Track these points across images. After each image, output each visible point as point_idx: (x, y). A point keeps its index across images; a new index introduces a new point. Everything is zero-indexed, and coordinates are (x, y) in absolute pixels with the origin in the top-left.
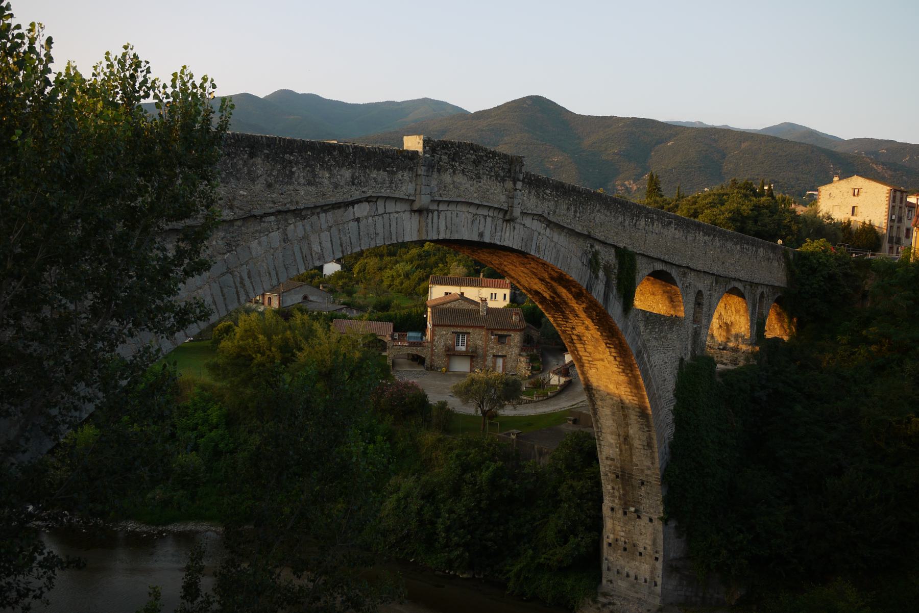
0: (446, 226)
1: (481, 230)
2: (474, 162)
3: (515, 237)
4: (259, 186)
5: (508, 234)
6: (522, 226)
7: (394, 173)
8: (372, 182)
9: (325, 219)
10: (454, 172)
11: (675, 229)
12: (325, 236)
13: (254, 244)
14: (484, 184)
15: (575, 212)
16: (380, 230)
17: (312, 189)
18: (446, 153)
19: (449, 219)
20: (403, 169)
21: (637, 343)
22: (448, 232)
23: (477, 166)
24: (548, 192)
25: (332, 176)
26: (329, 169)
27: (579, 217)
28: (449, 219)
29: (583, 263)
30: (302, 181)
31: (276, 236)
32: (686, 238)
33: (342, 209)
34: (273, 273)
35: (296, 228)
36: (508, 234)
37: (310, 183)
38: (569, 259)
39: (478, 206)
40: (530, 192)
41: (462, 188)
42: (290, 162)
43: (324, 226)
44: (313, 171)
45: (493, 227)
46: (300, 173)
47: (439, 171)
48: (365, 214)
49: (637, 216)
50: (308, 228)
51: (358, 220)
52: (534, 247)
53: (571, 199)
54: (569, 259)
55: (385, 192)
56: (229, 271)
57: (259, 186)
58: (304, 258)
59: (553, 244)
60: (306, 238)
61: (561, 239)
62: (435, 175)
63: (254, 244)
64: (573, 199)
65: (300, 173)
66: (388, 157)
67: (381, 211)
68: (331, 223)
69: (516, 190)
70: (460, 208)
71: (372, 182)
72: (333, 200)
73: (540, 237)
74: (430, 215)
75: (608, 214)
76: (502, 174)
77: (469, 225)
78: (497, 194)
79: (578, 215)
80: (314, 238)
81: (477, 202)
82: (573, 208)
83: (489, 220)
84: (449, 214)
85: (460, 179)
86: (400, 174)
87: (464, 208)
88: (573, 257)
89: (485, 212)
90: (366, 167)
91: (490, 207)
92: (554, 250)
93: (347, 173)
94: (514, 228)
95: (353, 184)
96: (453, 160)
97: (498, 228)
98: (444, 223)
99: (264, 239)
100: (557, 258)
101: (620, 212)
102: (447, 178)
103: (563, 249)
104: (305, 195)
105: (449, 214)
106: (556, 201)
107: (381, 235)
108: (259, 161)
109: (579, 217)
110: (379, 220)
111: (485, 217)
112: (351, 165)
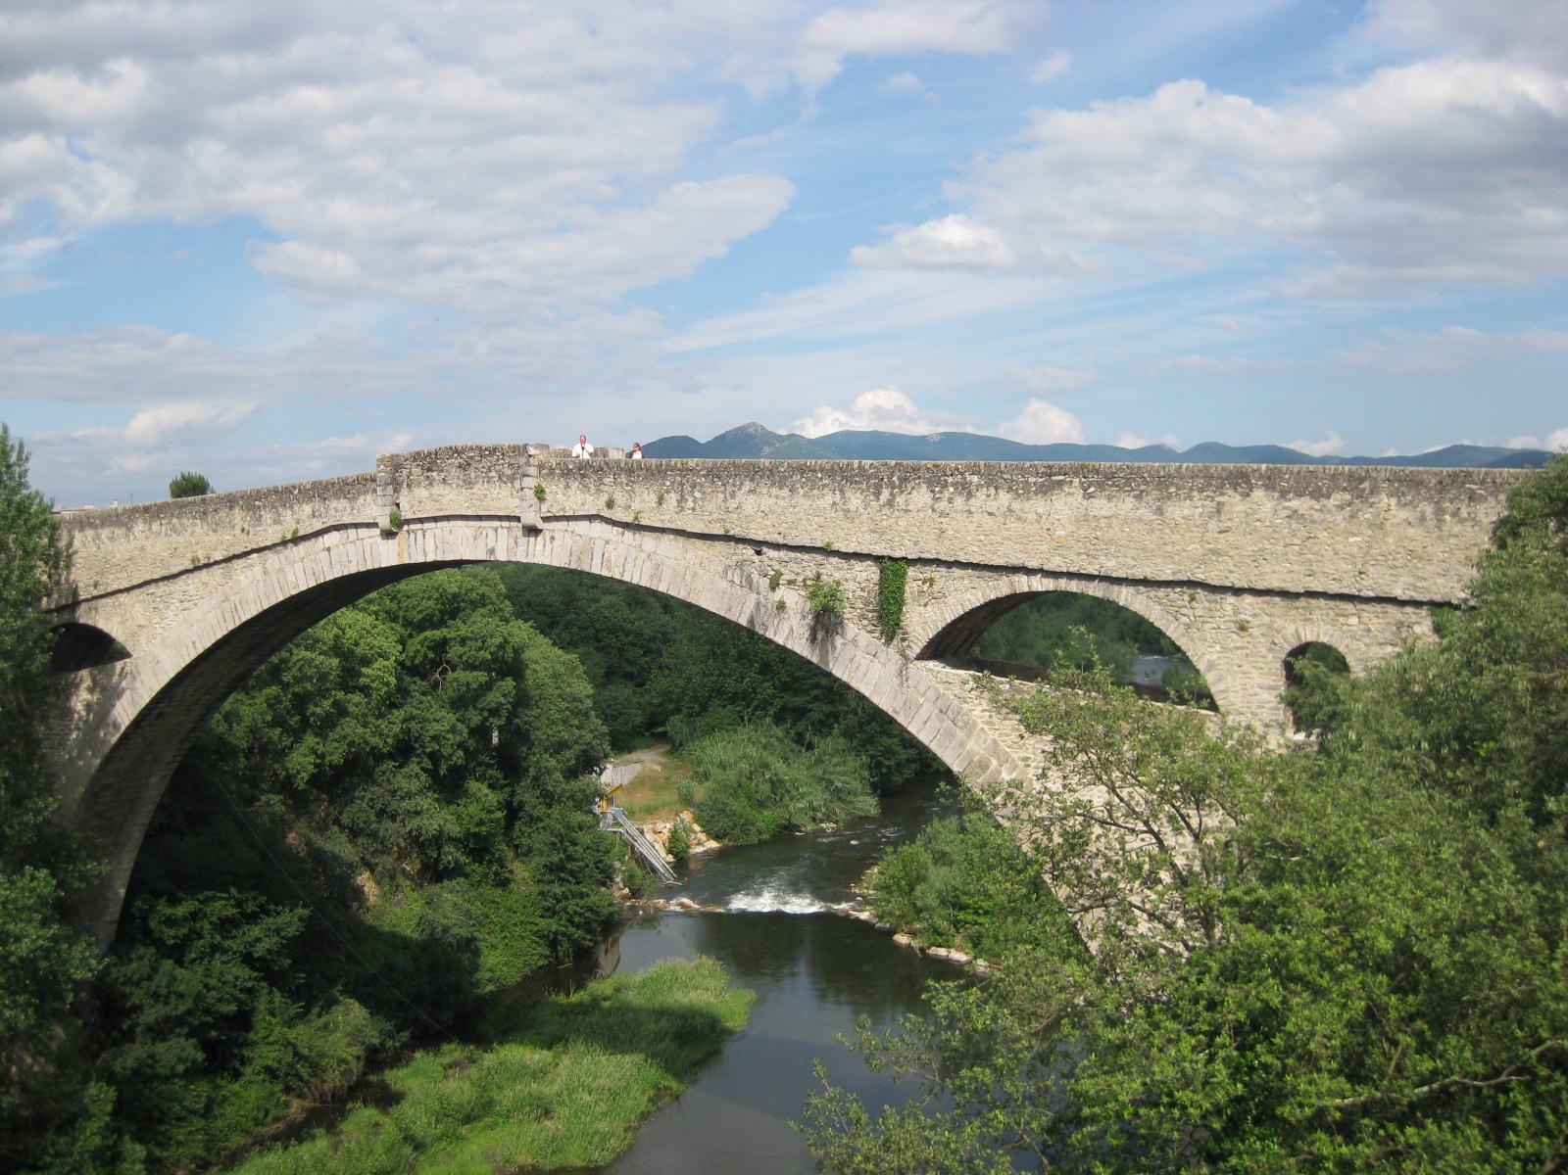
0: (436, 547)
1: (490, 546)
2: (460, 467)
3: (555, 550)
4: (238, 530)
5: (539, 547)
7: (355, 499)
10: (431, 484)
11: (1088, 496)
13: (242, 577)
14: (479, 489)
15: (682, 500)
17: (278, 527)
18: (418, 465)
21: (962, 745)
22: (439, 552)
23: (465, 470)
24: (606, 480)
26: (291, 508)
27: (693, 509)
29: (732, 581)
30: (269, 521)
31: (258, 569)
32: (1160, 511)
33: (313, 540)
34: (258, 601)
36: (539, 547)
37: (277, 522)
38: (688, 577)
40: (567, 486)
41: (444, 500)
42: (259, 507)
44: (277, 511)
45: (512, 540)
47: (409, 486)
48: (336, 542)
49: (892, 486)
50: (283, 560)
51: (329, 549)
52: (597, 561)
53: (668, 483)
54: (688, 577)
55: (346, 520)
56: (226, 599)
59: (644, 556)
60: (281, 570)
62: (404, 491)
64: (672, 483)
66: (347, 484)
69: (522, 489)
73: (610, 547)
74: (412, 535)
75: (785, 492)
76: (508, 472)
77: (471, 539)
79: (690, 504)
80: (288, 569)
82: (672, 499)
85: (437, 490)
86: (361, 499)
88: (701, 572)
89: (496, 524)
90: (325, 499)
93: (307, 508)
94: (553, 538)
95: (314, 516)
96: (429, 470)
98: (432, 543)
99: (249, 573)
101: (824, 486)
102: (421, 493)
103: (668, 562)
104: (271, 534)
105: (438, 531)
106: (627, 491)
107: (354, 562)
108: (237, 510)
109: (693, 509)
110: (351, 548)
112: (310, 499)
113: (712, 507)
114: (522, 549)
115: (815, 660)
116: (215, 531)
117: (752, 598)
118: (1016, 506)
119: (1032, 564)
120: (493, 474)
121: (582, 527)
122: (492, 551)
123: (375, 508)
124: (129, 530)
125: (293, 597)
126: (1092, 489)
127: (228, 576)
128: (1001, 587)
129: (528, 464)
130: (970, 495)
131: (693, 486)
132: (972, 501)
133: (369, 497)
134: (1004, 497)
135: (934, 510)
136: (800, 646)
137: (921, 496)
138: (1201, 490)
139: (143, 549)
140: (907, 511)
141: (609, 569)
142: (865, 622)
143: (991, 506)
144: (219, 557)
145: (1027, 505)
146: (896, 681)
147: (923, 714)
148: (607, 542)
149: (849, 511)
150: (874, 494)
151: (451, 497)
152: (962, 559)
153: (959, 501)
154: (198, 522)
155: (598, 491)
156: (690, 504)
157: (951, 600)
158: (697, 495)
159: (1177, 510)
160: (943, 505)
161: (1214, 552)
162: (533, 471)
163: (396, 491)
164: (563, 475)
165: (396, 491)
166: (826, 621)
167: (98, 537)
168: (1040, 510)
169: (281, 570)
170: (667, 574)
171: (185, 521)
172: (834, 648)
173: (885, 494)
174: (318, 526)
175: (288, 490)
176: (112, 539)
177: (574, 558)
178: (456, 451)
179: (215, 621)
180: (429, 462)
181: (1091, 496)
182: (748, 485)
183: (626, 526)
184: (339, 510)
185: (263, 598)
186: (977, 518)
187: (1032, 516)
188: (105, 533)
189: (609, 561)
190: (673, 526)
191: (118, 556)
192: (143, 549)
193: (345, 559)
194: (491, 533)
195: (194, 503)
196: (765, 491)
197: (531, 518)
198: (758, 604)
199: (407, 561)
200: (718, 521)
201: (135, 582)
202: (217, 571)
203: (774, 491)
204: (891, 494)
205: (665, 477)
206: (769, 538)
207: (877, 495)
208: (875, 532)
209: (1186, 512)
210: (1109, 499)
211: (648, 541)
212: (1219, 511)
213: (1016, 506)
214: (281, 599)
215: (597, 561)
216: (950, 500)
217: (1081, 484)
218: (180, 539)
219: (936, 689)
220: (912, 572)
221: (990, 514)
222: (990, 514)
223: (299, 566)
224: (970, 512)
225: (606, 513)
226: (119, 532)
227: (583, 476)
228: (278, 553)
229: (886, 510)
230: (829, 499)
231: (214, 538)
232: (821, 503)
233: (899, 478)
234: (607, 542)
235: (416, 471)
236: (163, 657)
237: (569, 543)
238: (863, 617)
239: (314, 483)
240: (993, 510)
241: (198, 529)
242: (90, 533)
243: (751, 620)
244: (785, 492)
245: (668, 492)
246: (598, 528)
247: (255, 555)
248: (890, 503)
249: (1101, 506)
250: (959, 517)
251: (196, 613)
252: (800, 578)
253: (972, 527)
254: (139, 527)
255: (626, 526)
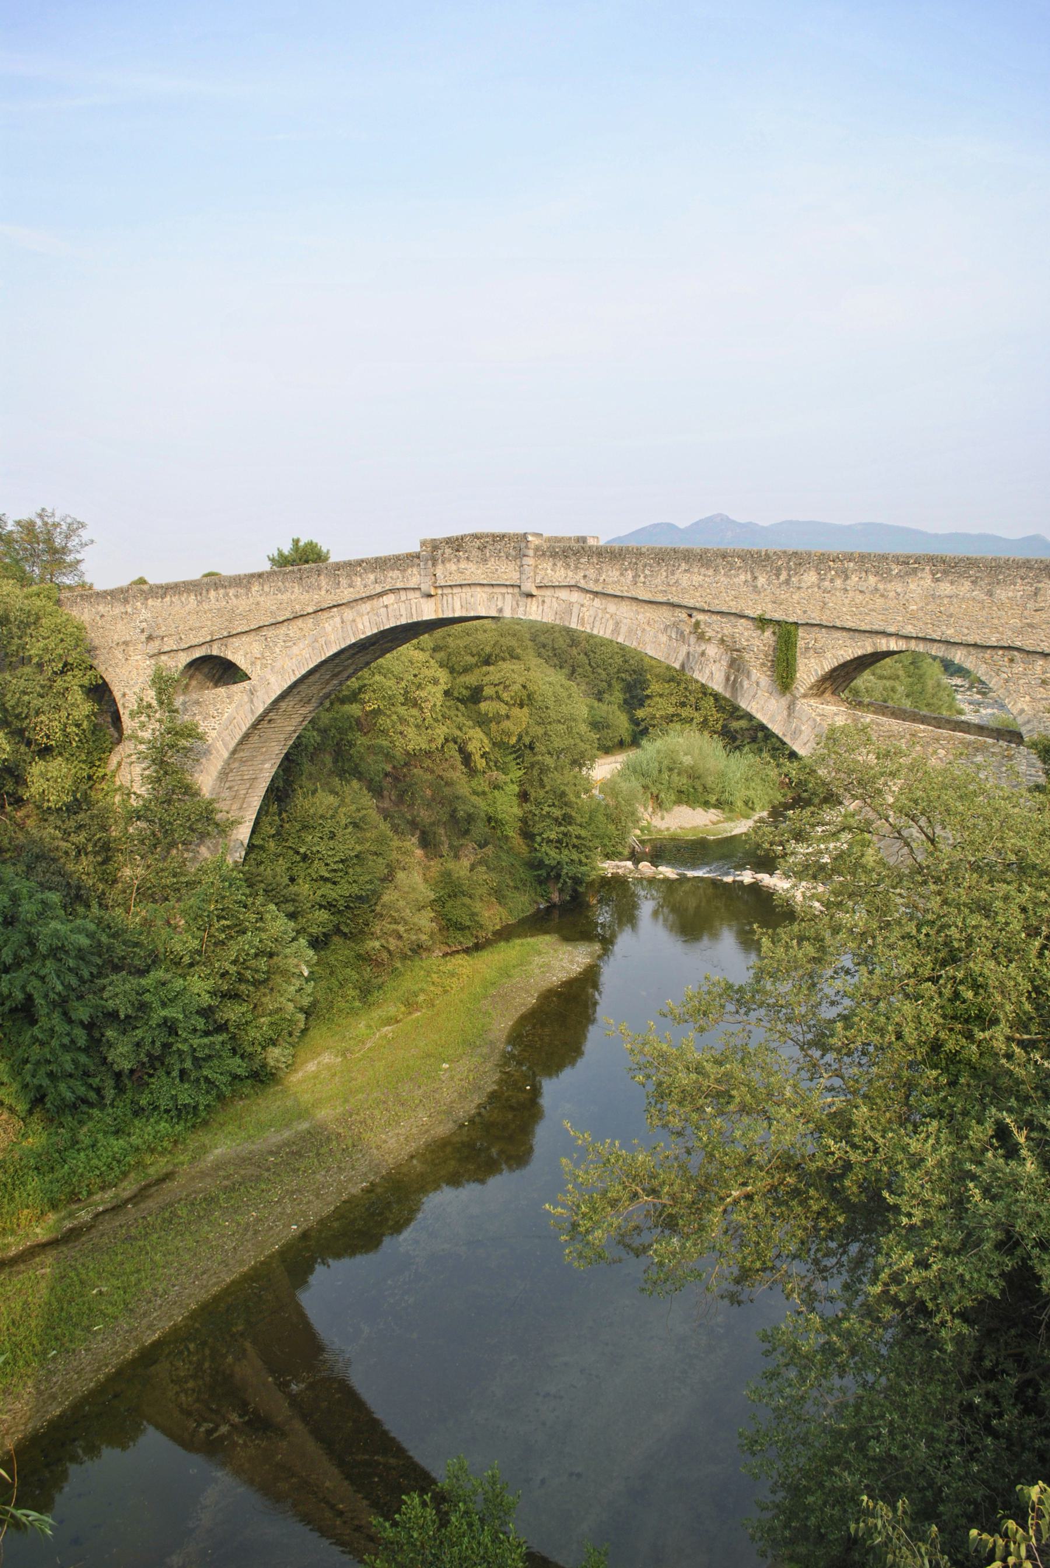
4: (323, 592)
6: (554, 600)
7: (405, 570)
8: (389, 580)
9: (366, 607)
12: (366, 618)
13: (327, 625)
15: (636, 576)
16: (403, 612)
19: (464, 601)
20: (412, 566)
22: (464, 610)
24: (582, 560)
25: (362, 579)
26: (360, 576)
27: (644, 583)
28: (464, 601)
31: (338, 619)
32: (990, 594)
35: (348, 614)
36: (534, 608)
37: (350, 586)
38: (639, 633)
39: (492, 585)
40: (555, 564)
43: (365, 612)
46: (344, 581)
47: (443, 562)
51: (386, 607)
52: (574, 619)
54: (639, 633)
55: (399, 585)
56: (316, 641)
57: (323, 592)
58: (354, 634)
59: (608, 616)
60: (354, 621)
61: (625, 611)
63: (327, 625)
65: (344, 581)
67: (403, 598)
68: (369, 609)
70: (473, 589)
71: (389, 580)
72: (364, 595)
73: (585, 609)
78: (508, 572)
79: (642, 579)
80: (358, 620)
81: (485, 582)
82: (630, 574)
83: (509, 597)
84: (463, 595)
85: (463, 565)
86: (409, 571)
87: (478, 589)
88: (648, 628)
89: (504, 590)
91: (506, 586)
92: (611, 622)
93: (372, 577)
94: (543, 602)
96: (458, 551)
97: (520, 603)
100: (616, 630)
102: (452, 567)
105: (463, 595)
108: (322, 577)
109: (644, 583)
110: (402, 606)
111: (503, 594)
112: (373, 571)
113: (658, 581)
114: (521, 609)
115: (728, 695)
116: (308, 592)
117: (684, 649)
118: (881, 586)
119: (892, 629)
120: (502, 554)
121: (563, 594)
122: (501, 610)
123: (415, 577)
124: (249, 589)
125: (361, 640)
126: (939, 575)
127: (317, 624)
128: (865, 647)
129: (527, 547)
130: (847, 578)
131: (645, 566)
132: (848, 582)
133: (415, 570)
134: (872, 580)
135: (819, 588)
136: (717, 685)
137: (811, 577)
138: (1022, 579)
139: (258, 603)
140: (799, 588)
141: (583, 625)
142: (765, 669)
143: (863, 586)
144: (311, 611)
145: (889, 586)
146: (785, 713)
147: (804, 737)
148: (582, 606)
149: (756, 587)
150: (775, 574)
151: (474, 571)
152: (838, 624)
153: (838, 582)
154: (296, 585)
155: (577, 568)
156: (642, 579)
157: (829, 655)
158: (647, 572)
159: (1002, 594)
160: (827, 583)
161: (1030, 625)
162: (531, 553)
163: (434, 565)
164: (551, 556)
165: (434, 565)
166: (736, 666)
167: (227, 594)
168: (899, 590)
169: (354, 621)
170: (624, 629)
171: (287, 584)
172: (742, 686)
173: (783, 577)
174: (379, 590)
175: (360, 563)
176: (236, 596)
177: (558, 617)
178: (476, 537)
179: (308, 656)
180: (457, 544)
181: (938, 580)
182: (684, 566)
183: (596, 594)
184: (394, 578)
185: (341, 640)
186: (851, 594)
187: (892, 594)
188: (232, 592)
189: (583, 619)
190: (629, 595)
191: (241, 608)
192: (258, 603)
193: (398, 613)
194: (500, 597)
195: (293, 572)
196: (696, 570)
197: (529, 587)
198: (688, 653)
199: (441, 616)
200: (662, 591)
201: (252, 627)
202: (310, 621)
203: (703, 570)
204: (789, 575)
205: (624, 559)
206: (698, 605)
207: (778, 576)
208: (774, 603)
209: (1010, 594)
210: (952, 583)
211: (612, 607)
212: (1036, 594)
213: (881, 586)
214: (353, 641)
215: (574, 619)
216: (832, 581)
217: (931, 571)
218: (284, 597)
219: (814, 720)
220: (801, 632)
221: (861, 592)
222: (861, 592)
223: (366, 618)
224: (846, 590)
225: (582, 584)
226: (242, 591)
227: (566, 557)
228: (352, 608)
229: (784, 587)
230: (743, 577)
231: (306, 596)
232: (736, 580)
233: (795, 564)
234: (582, 606)
235: (448, 551)
236: (272, 680)
237: (555, 605)
238: (763, 665)
239: (377, 558)
240: (863, 589)
241: (296, 590)
242: (222, 591)
243: (683, 666)
244: (711, 572)
245: (626, 570)
246: (575, 596)
247: (335, 609)
248: (787, 582)
249: (946, 588)
250: (838, 594)
251: (295, 650)
252: (719, 636)
253: (846, 601)
254: (255, 588)
255: (596, 594)
